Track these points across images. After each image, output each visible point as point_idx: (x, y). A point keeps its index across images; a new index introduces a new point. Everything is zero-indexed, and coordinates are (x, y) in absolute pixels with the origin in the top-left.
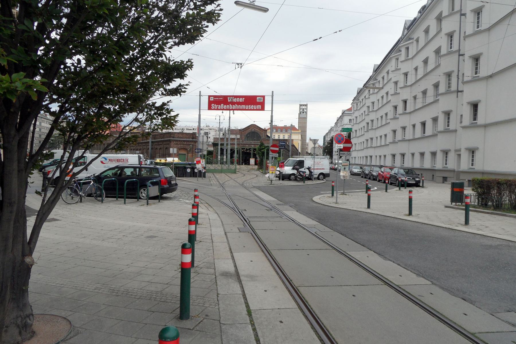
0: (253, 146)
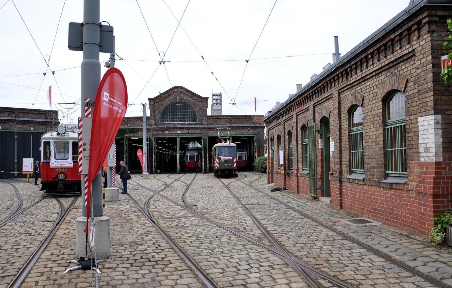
0: (179, 132)
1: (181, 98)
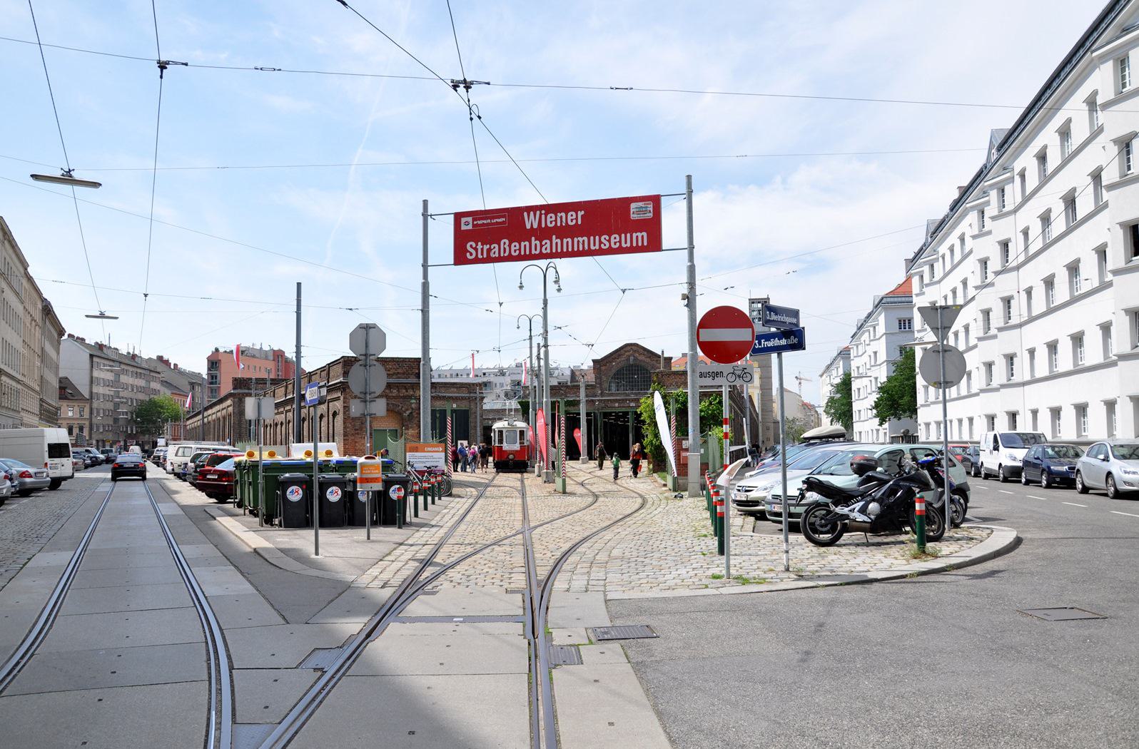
1: (636, 359)
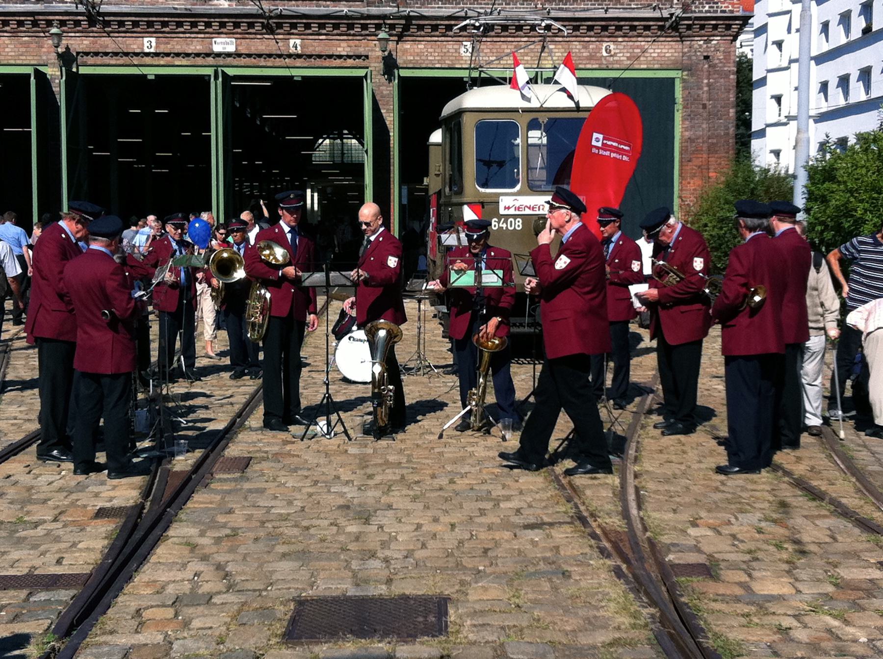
0: (223, 44)
